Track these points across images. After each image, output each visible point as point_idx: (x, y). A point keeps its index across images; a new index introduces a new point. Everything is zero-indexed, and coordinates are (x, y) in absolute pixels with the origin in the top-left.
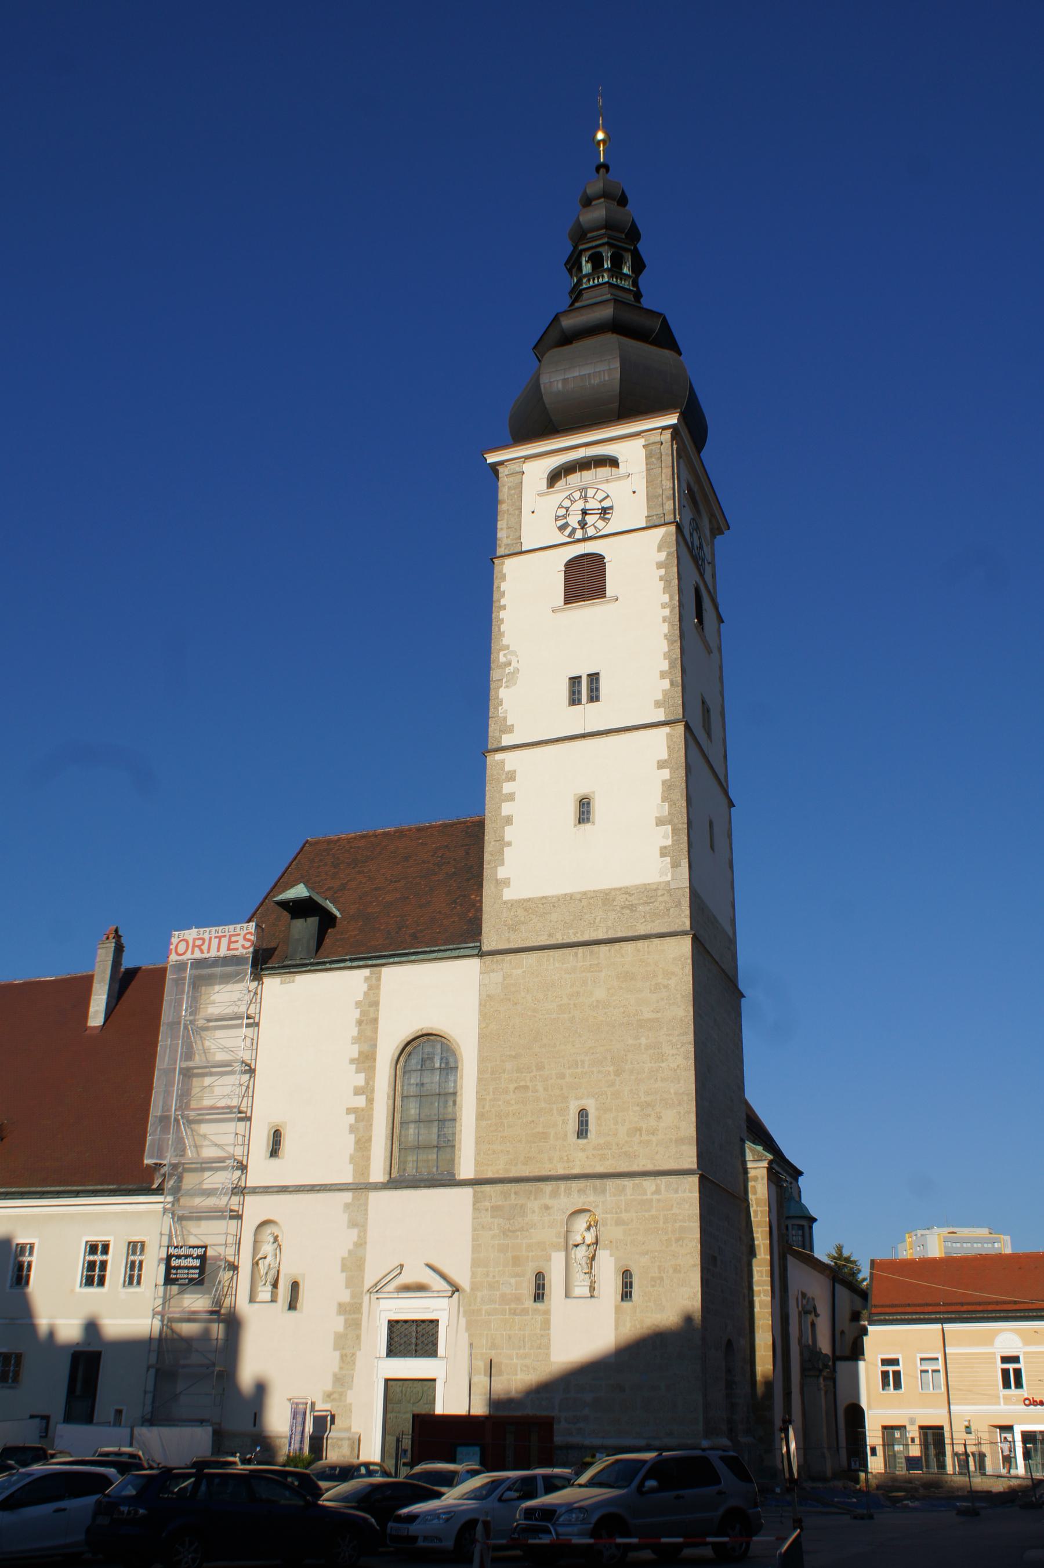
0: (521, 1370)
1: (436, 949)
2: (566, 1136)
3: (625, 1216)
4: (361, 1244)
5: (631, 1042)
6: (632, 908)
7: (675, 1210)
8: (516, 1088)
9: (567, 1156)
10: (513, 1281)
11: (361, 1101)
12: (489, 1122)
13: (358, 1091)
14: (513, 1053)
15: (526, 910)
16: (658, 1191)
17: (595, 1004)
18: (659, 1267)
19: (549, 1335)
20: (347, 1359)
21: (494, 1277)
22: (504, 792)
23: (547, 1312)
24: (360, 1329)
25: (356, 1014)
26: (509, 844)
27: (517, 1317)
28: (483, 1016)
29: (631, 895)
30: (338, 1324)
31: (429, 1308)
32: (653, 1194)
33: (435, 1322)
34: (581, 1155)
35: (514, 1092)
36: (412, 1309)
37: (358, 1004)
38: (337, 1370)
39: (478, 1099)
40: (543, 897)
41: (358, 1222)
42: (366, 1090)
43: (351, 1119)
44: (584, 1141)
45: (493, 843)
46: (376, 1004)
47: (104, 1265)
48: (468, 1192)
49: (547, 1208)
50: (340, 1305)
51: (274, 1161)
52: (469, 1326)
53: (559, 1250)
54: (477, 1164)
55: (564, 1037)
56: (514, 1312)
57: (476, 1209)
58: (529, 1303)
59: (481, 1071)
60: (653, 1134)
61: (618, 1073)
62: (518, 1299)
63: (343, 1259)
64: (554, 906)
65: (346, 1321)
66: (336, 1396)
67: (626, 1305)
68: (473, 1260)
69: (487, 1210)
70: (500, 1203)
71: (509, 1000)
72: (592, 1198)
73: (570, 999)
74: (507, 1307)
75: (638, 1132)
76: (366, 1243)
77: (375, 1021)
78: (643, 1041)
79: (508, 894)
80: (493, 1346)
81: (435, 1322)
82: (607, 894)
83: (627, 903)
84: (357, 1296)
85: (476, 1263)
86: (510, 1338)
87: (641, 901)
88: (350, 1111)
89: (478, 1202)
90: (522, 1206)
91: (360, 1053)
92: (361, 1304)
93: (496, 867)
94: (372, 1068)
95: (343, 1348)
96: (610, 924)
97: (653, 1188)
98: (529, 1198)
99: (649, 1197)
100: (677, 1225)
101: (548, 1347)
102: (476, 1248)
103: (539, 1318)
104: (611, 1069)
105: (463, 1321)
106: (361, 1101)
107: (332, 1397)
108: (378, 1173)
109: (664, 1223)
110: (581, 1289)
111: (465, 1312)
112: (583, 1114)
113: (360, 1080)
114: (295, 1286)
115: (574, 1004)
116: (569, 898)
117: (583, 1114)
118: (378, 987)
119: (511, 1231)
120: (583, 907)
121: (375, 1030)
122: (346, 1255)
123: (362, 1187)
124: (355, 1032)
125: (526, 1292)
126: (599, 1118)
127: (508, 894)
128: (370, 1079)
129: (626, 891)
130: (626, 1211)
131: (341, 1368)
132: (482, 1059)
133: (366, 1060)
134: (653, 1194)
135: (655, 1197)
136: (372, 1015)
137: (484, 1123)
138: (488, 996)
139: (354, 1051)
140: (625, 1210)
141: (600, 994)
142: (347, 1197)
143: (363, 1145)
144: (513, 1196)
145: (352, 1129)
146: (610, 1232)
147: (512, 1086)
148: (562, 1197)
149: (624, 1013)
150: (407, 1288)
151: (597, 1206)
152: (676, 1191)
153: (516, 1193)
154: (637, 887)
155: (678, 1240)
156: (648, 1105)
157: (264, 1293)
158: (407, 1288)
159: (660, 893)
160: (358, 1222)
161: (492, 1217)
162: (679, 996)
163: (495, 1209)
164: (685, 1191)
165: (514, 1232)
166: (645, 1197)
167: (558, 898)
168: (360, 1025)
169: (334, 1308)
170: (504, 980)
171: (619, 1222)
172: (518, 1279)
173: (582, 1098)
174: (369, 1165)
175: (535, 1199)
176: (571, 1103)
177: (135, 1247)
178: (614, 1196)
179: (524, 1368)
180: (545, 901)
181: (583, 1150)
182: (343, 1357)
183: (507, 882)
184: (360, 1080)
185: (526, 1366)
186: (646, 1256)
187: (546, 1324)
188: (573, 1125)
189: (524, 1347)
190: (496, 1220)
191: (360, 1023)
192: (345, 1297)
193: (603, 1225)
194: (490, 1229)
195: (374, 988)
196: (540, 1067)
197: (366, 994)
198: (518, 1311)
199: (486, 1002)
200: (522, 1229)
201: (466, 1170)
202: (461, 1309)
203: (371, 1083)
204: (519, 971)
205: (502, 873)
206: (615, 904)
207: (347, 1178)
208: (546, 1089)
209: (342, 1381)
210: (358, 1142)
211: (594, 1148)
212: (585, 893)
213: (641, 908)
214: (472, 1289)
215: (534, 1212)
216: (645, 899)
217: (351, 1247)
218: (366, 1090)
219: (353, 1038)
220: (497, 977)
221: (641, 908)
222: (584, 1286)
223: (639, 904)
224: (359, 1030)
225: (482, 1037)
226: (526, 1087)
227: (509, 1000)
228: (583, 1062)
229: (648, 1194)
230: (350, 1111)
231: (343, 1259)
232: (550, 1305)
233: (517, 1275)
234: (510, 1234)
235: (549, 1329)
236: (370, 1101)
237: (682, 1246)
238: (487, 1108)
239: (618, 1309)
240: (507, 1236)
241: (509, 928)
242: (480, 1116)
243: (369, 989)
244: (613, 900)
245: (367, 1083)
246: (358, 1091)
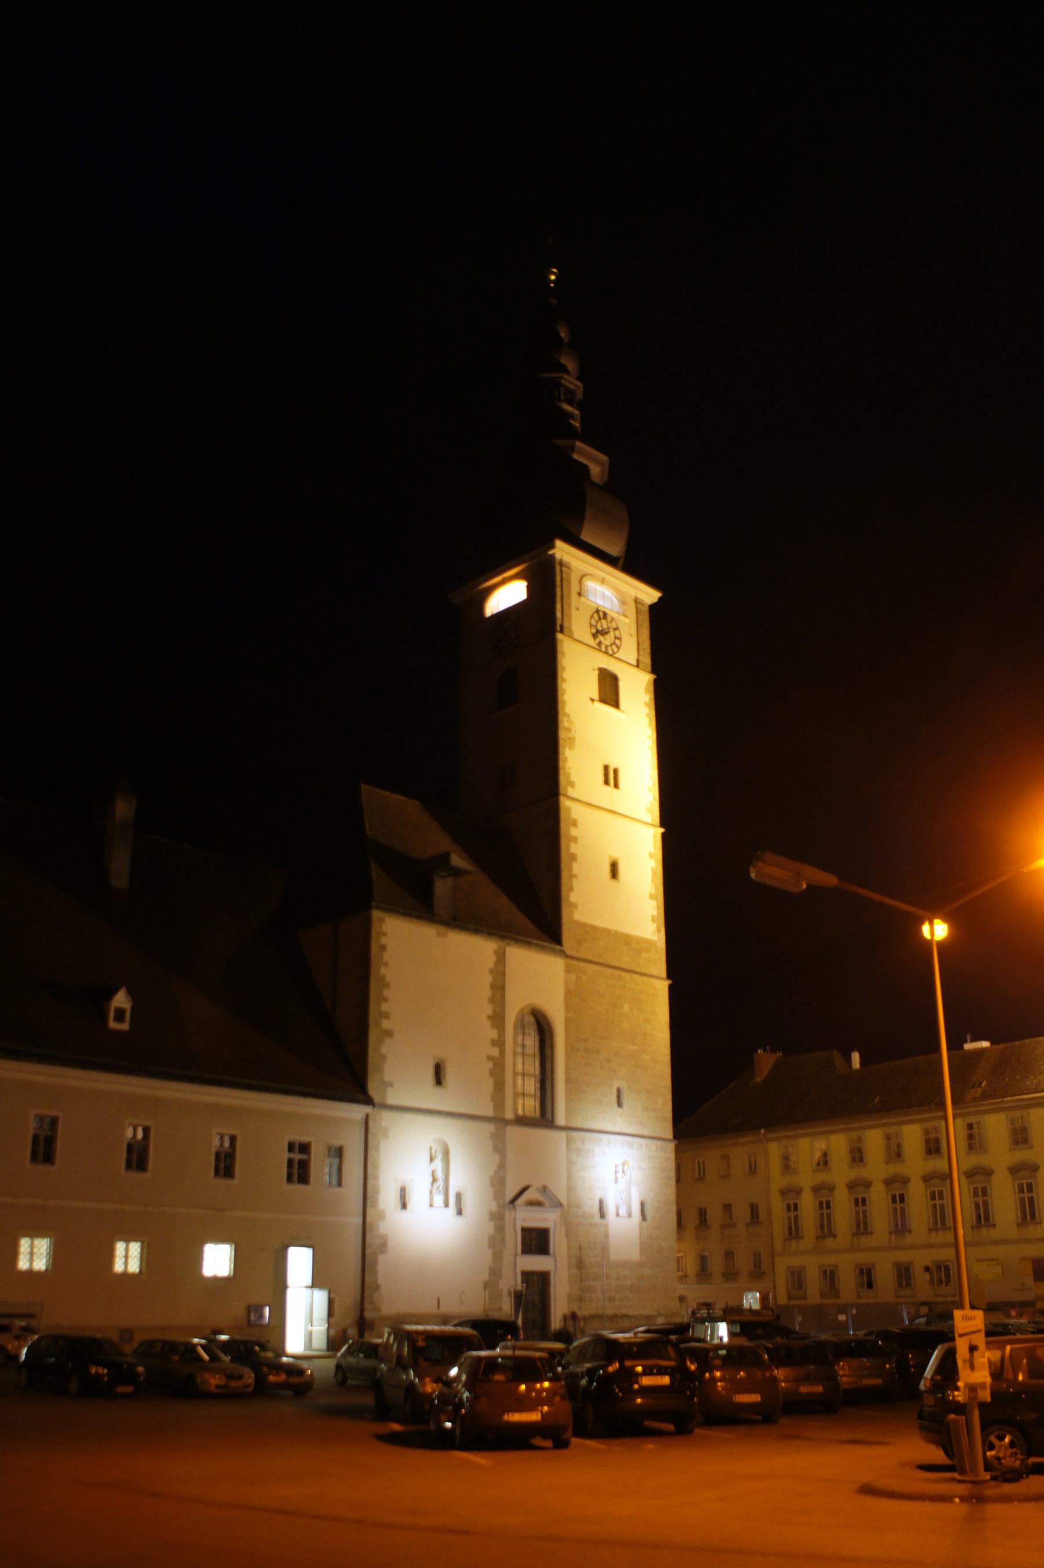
13: (494, 1043)
25: (488, 979)
36: (536, 1219)
42: (499, 1043)
43: (490, 1065)
67: (644, 1222)
77: (503, 988)
84: (501, 1207)
88: (490, 1058)
91: (494, 1012)
106: (495, 1052)
112: (619, 1091)
113: (494, 1034)
121: (503, 996)
132: (567, 1037)
133: (498, 1019)
139: (488, 1009)
142: (490, 1127)
145: (492, 1073)
160: (500, 1148)
167: (604, 930)
182: (494, 1254)
184: (494, 1034)
195: (501, 958)
197: (496, 964)
199: (568, 993)
207: (489, 1112)
225: (568, 1020)
230: (490, 1058)
236: (502, 1052)
246: (494, 1043)
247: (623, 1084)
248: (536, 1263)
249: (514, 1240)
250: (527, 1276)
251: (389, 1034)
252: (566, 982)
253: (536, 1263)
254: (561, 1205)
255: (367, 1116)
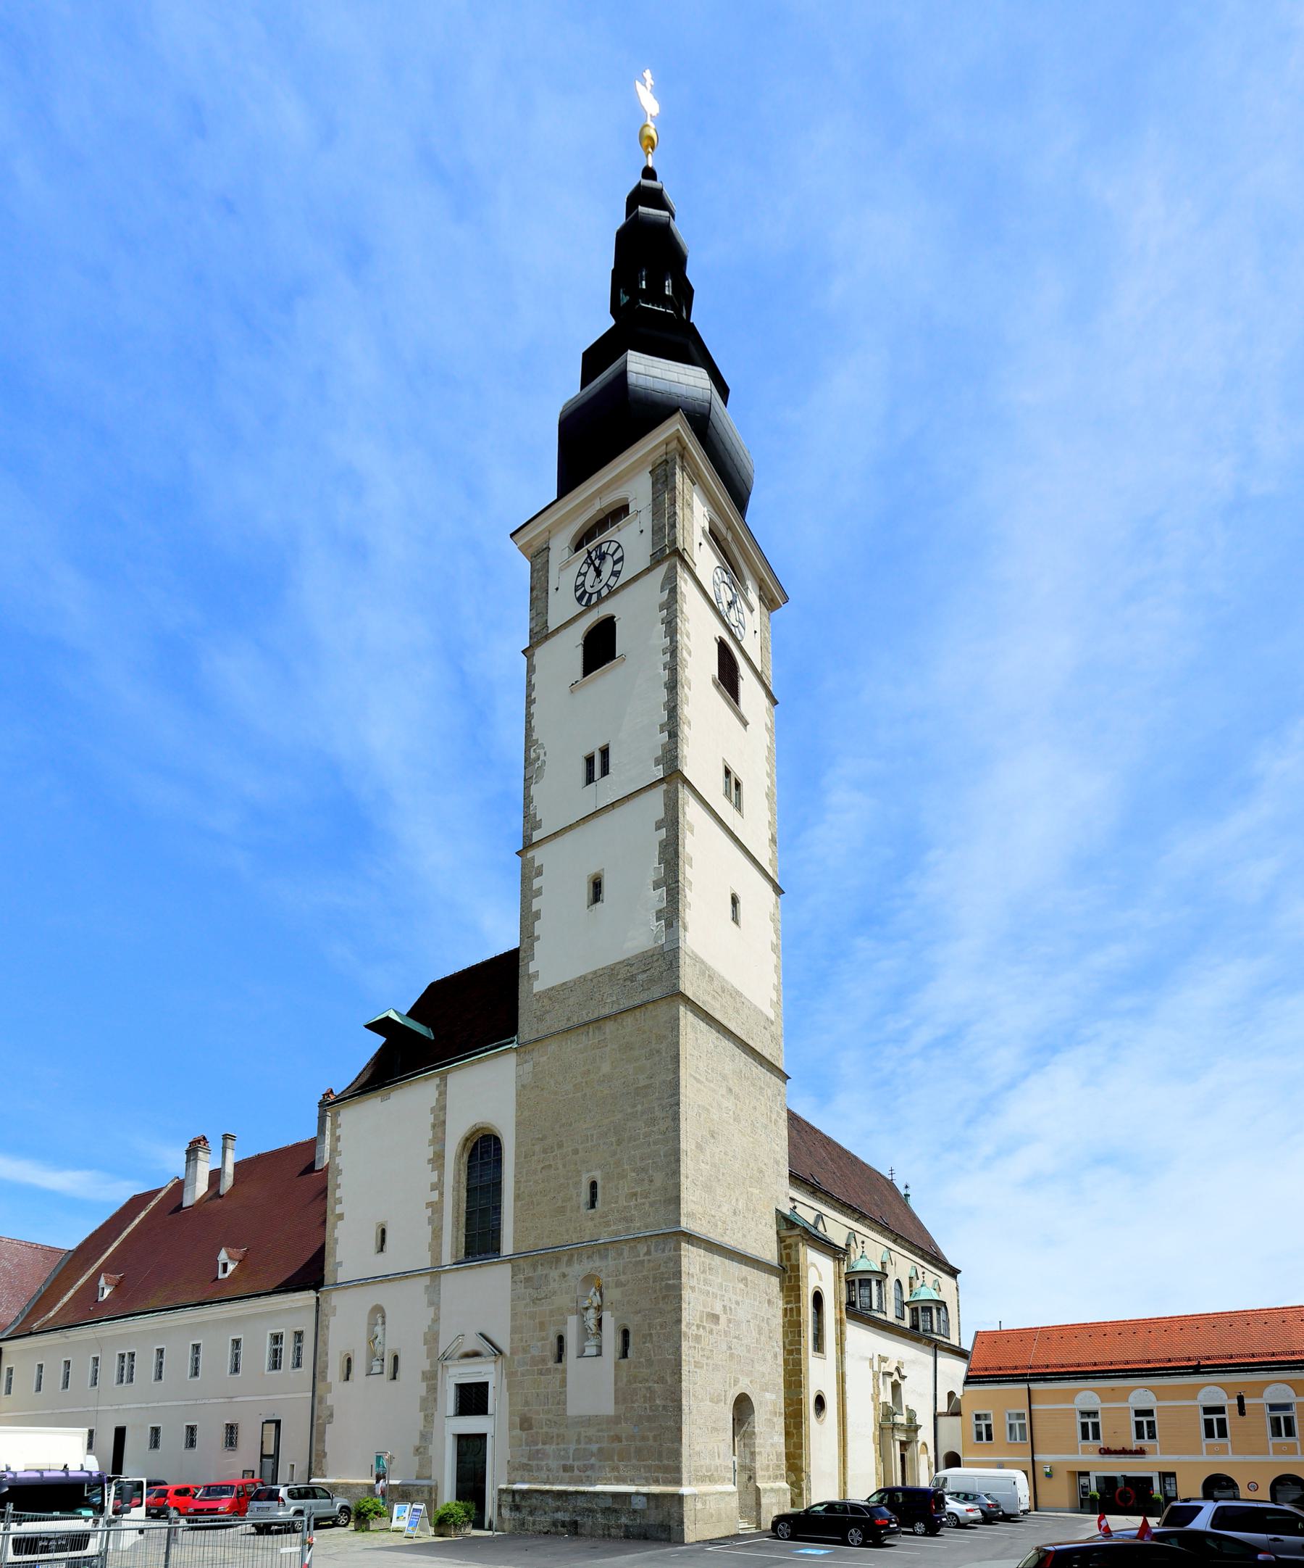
0: (546, 1424)
1: (484, 1048)
2: (579, 1207)
3: (623, 1278)
4: (436, 1320)
5: (629, 1110)
6: (632, 978)
7: (663, 1269)
8: (543, 1168)
9: (580, 1226)
10: (539, 1344)
11: (435, 1196)
12: (523, 1202)
14: (540, 1136)
15: (550, 999)
16: (648, 1253)
17: (601, 1079)
18: (649, 1324)
19: (565, 1391)
20: (429, 1419)
21: (526, 1341)
22: (534, 889)
23: (564, 1371)
24: (436, 1392)
26: (538, 938)
27: (542, 1377)
28: (520, 1105)
29: (631, 965)
30: (422, 1389)
31: (481, 1372)
32: (645, 1254)
33: (486, 1384)
34: (590, 1224)
35: (541, 1172)
37: (432, 1109)
38: (422, 1428)
39: (516, 1182)
40: (564, 983)
41: (434, 1303)
44: (593, 1211)
45: (526, 940)
46: (443, 1108)
47: (281, 1349)
48: (507, 1269)
49: (564, 1275)
50: (423, 1373)
51: (382, 1255)
52: (510, 1387)
53: (572, 1314)
54: (516, 1240)
55: (578, 1114)
56: (541, 1373)
57: (514, 1282)
58: (551, 1364)
59: (517, 1157)
60: (646, 1197)
61: (619, 1142)
62: (543, 1361)
63: (425, 1333)
64: (571, 991)
65: (427, 1386)
66: (421, 1450)
67: (623, 1361)
68: (512, 1327)
69: (521, 1282)
70: (530, 1275)
71: (538, 1087)
72: (597, 1264)
73: (582, 1078)
74: (535, 1368)
75: (634, 1197)
76: (439, 1318)
78: (639, 1107)
79: (538, 987)
80: (527, 1403)
81: (486, 1384)
82: (612, 970)
83: (629, 974)
85: (514, 1330)
86: (538, 1396)
87: (641, 970)
88: (429, 1205)
89: (515, 1275)
90: (546, 1275)
92: (437, 1371)
93: (528, 962)
94: (443, 1165)
95: (426, 1410)
96: (614, 999)
97: (645, 1249)
98: (551, 1268)
99: (641, 1258)
100: (664, 1283)
101: (565, 1404)
102: (514, 1316)
103: (558, 1376)
104: (613, 1139)
105: (505, 1381)
106: (435, 1196)
107: (420, 1450)
108: (447, 1258)
109: (653, 1282)
110: (591, 1350)
111: (506, 1374)
112: (594, 1185)
113: (434, 1177)
114: (396, 1358)
115: (586, 1082)
116: (583, 979)
117: (594, 1185)
118: (445, 1093)
119: (540, 1299)
120: (594, 987)
122: (427, 1330)
123: (435, 1272)
124: (430, 1135)
125: (549, 1354)
126: (604, 1188)
127: (538, 987)
128: (441, 1176)
129: (628, 963)
130: (624, 1273)
131: (425, 1426)
133: (438, 1160)
134: (645, 1254)
135: (646, 1258)
136: (442, 1118)
137: (519, 1204)
138: (523, 1086)
140: (623, 1272)
141: (606, 1068)
142: (426, 1281)
143: (437, 1234)
144: (539, 1266)
145: (431, 1221)
146: (612, 1294)
147: (539, 1167)
148: (575, 1265)
149: (624, 1083)
150: (467, 1355)
151: (601, 1270)
152: (663, 1251)
153: (542, 1265)
154: (636, 957)
155: (664, 1298)
156: (644, 1170)
157: (377, 1369)
158: (467, 1355)
159: (655, 959)
160: (434, 1303)
161: (525, 1288)
162: (669, 1059)
163: (528, 1280)
164: (670, 1250)
165: (540, 1299)
166: (638, 1259)
167: (575, 982)
168: (434, 1128)
169: (420, 1376)
170: (534, 1069)
171: (619, 1284)
172: (543, 1342)
173: (591, 1171)
174: (441, 1251)
175: (556, 1268)
176: (583, 1176)
177: (299, 1335)
178: (615, 1260)
179: (548, 1423)
180: (565, 987)
181: (592, 1219)
182: (426, 1416)
183: (536, 975)
184: (434, 1177)
185: (549, 1420)
186: (639, 1315)
187: (564, 1383)
188: (585, 1196)
189: (548, 1403)
190: (528, 1290)
191: (434, 1126)
192: (426, 1366)
193: (606, 1288)
194: (524, 1299)
196: (560, 1146)
197: (437, 1100)
198: (544, 1371)
199: (522, 1090)
200: (546, 1297)
201: (507, 1247)
202: (504, 1371)
203: (442, 1178)
204: (545, 1058)
205: (532, 968)
206: (619, 977)
208: (564, 1166)
209: (425, 1437)
210: (433, 1232)
211: (601, 1217)
212: (595, 972)
213: (640, 977)
214: (511, 1354)
215: (555, 1280)
216: (643, 967)
217: (430, 1324)
218: (438, 1186)
219: (430, 1141)
220: (528, 1067)
221: (640, 977)
222: (592, 1345)
223: (638, 974)
224: (433, 1133)
225: (518, 1124)
226: (550, 1165)
227: (538, 1087)
228: (592, 1135)
229: (641, 1255)
231: (425, 1333)
232: (566, 1364)
233: (543, 1339)
234: (538, 1302)
235: (566, 1386)
236: (441, 1194)
237: (667, 1303)
238: (522, 1189)
239: (617, 1366)
240: (536, 1304)
241: (538, 1020)
242: (517, 1197)
243: (439, 1096)
244: (618, 975)
245: (439, 1179)
247: (598, 1175)
248: (472, 1425)
249: (449, 1400)
250: (462, 1439)
251: (341, 1217)
252: (518, 1077)
253: (472, 1425)
254: (499, 1352)
255: (318, 1298)
